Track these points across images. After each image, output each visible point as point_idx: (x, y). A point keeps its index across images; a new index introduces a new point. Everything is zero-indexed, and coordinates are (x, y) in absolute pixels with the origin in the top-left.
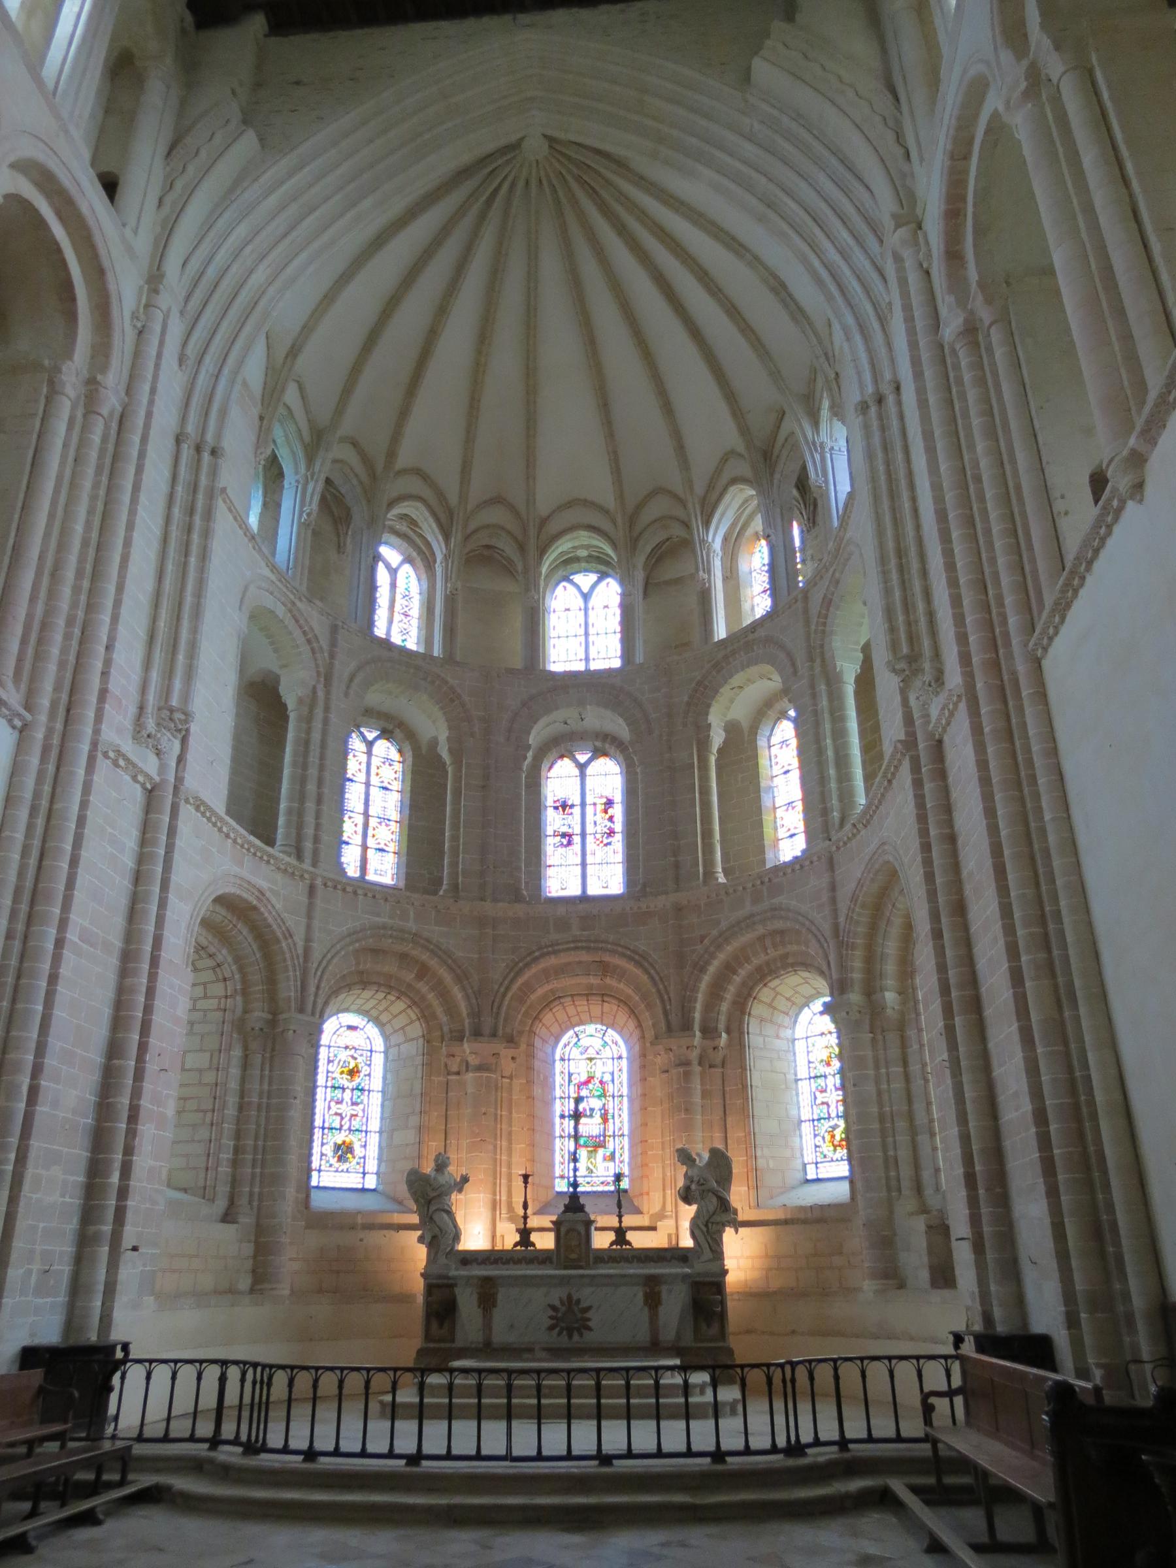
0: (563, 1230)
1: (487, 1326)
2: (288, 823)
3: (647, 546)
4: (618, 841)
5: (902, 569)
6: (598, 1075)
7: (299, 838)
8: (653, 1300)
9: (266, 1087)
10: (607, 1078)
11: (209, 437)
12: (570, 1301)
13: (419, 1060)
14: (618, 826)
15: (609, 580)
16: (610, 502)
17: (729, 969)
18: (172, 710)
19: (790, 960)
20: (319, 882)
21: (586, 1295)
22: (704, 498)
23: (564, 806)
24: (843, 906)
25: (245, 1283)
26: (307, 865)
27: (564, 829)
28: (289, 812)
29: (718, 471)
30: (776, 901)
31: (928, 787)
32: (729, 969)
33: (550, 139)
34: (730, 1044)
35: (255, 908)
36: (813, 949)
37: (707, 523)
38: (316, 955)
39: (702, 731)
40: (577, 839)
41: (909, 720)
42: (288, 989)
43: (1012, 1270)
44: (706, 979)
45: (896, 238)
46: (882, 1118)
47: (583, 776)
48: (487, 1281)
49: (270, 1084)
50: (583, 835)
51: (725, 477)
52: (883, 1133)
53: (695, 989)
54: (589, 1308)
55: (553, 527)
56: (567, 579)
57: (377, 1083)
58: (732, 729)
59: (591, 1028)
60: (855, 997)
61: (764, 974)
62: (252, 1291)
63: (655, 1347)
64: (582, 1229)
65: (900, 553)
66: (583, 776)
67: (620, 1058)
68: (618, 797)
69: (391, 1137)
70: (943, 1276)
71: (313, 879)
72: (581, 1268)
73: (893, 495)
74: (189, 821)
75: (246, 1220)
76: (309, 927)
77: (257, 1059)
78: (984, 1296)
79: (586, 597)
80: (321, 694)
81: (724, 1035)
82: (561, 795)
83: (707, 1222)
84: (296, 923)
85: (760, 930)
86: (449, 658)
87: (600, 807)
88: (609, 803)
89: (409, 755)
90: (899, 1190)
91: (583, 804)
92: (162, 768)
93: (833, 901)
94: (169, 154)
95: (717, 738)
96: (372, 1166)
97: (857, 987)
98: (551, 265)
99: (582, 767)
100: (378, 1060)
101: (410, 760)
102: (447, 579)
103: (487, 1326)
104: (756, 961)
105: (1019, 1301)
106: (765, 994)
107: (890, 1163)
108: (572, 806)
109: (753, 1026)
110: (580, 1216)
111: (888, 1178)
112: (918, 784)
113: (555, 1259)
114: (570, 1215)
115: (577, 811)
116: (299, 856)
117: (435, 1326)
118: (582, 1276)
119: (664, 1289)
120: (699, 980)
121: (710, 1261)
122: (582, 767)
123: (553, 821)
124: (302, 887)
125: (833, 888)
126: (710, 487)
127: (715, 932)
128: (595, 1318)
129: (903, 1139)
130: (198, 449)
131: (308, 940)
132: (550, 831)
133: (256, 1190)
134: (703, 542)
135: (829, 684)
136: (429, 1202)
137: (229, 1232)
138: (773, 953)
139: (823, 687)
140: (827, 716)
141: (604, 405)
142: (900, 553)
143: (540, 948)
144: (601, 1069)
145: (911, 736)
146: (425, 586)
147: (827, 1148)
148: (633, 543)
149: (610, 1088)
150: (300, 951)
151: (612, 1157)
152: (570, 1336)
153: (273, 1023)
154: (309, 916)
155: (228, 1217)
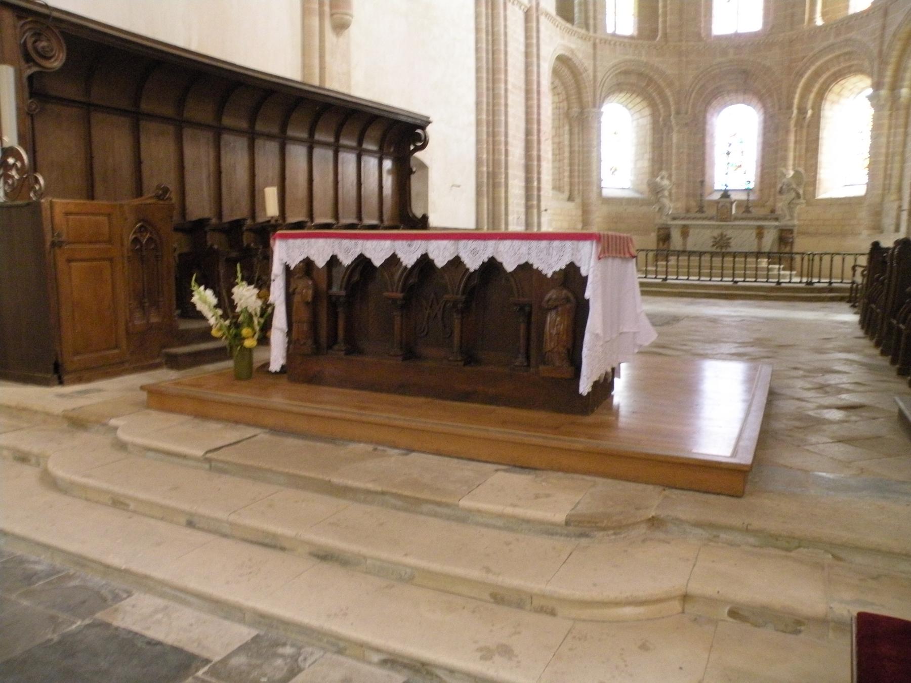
0: (720, 205)
1: (685, 244)
2: (580, 12)
7: (587, 19)
9: (581, 143)
12: (722, 236)
17: (817, 74)
19: (853, 69)
20: (598, 41)
21: (729, 233)
24: (888, 38)
26: (591, 33)
32: (817, 74)
34: (813, 115)
35: (570, 59)
36: (866, 64)
38: (599, 79)
42: (588, 98)
44: (803, 81)
46: (887, 155)
49: (583, 142)
52: (887, 162)
53: (796, 87)
54: (730, 239)
60: (884, 92)
61: (838, 76)
63: (758, 254)
64: (728, 205)
71: (595, 39)
72: (727, 221)
74: (545, 24)
75: (578, 200)
76: (595, 66)
77: (576, 130)
83: (789, 204)
84: (588, 63)
85: (837, 53)
90: (889, 189)
97: (887, 87)
103: (685, 244)
106: (836, 88)
107: (887, 176)
110: (727, 200)
111: (884, 185)
113: (715, 218)
114: (723, 200)
117: (661, 244)
118: (728, 225)
119: (766, 232)
120: (798, 82)
121: (789, 220)
127: (811, 54)
128: (733, 243)
129: (897, 166)
131: (595, 71)
133: (581, 188)
136: (658, 193)
137: (571, 205)
138: (843, 65)
143: (711, 66)
150: (591, 77)
152: (721, 249)
153: (582, 113)
154: (595, 58)
155: (570, 199)
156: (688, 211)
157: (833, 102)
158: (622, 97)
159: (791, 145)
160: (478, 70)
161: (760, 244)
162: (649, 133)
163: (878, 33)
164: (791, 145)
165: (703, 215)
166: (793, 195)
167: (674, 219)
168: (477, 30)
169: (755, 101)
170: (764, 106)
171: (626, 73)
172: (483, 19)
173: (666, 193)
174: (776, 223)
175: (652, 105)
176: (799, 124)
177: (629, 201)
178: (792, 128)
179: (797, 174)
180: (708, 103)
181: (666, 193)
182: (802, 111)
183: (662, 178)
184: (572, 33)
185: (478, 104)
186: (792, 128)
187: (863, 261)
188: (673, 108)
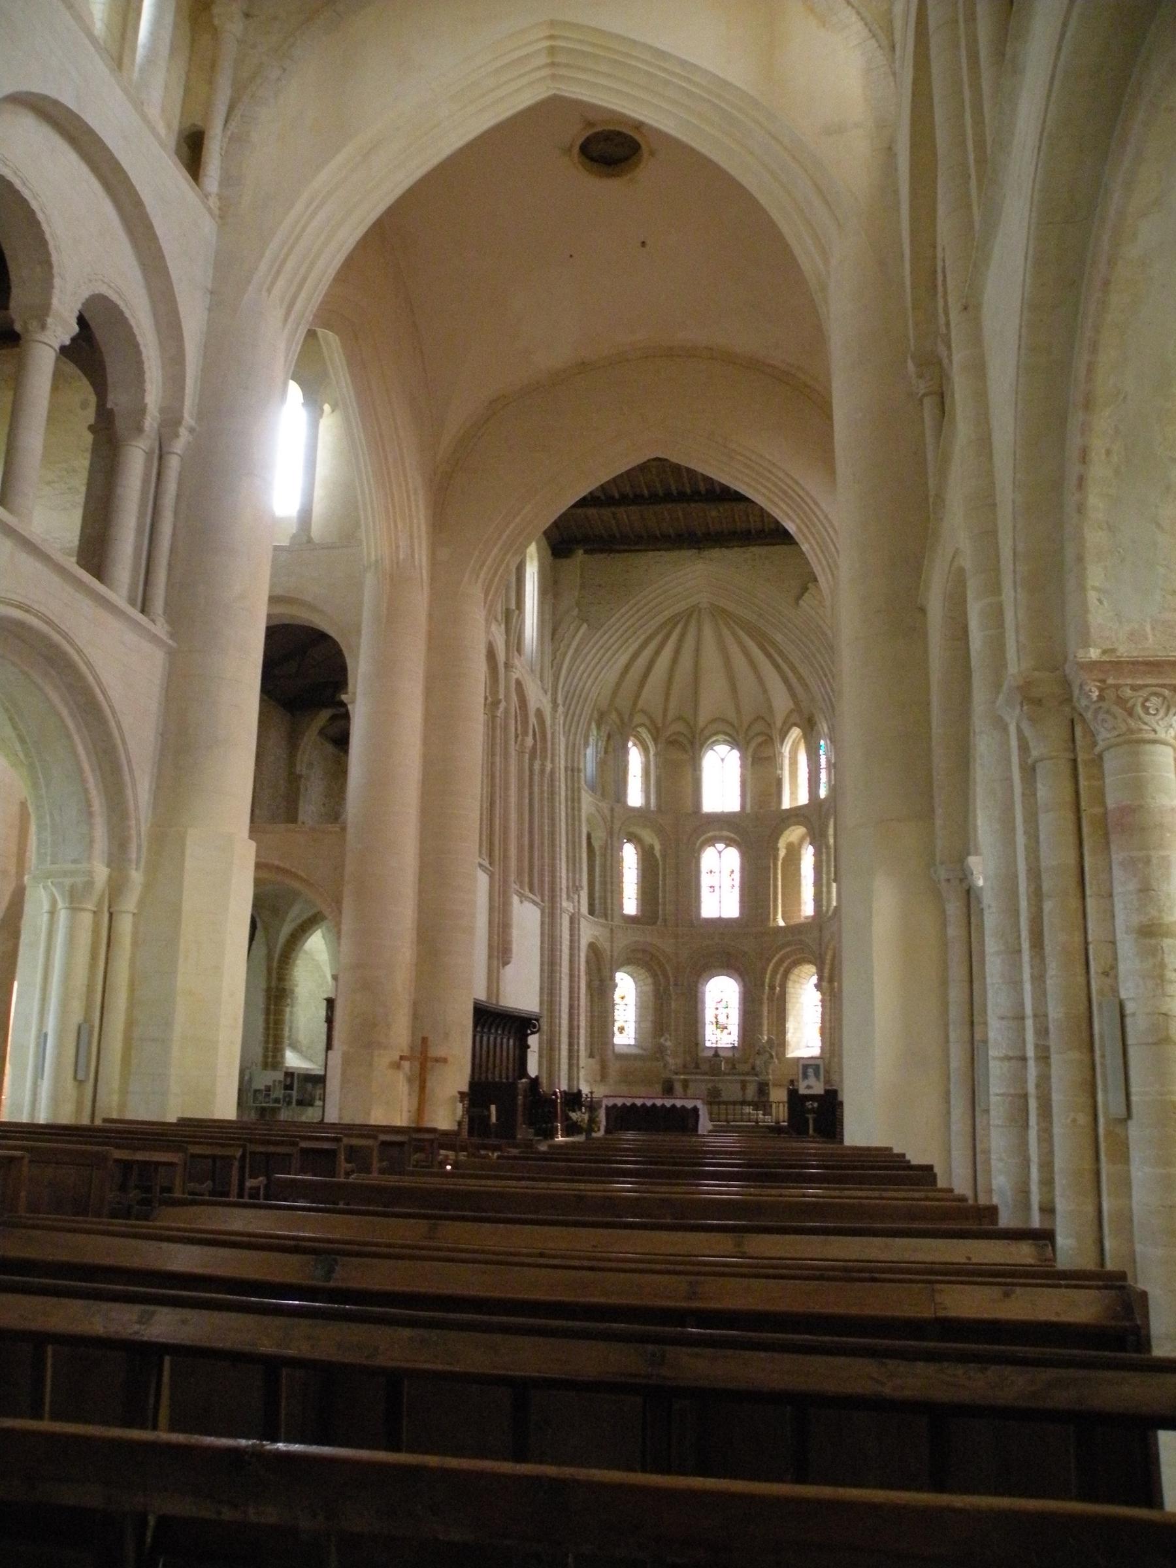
3: (753, 745)
7: (606, 909)
8: (744, 1088)
11: (576, 765)
13: (650, 994)
17: (781, 961)
18: (577, 887)
21: (720, 1086)
22: (782, 729)
25: (598, 1078)
28: (600, 898)
29: (788, 716)
32: (781, 961)
33: (712, 604)
34: (780, 991)
38: (615, 957)
40: (717, 889)
46: (830, 1028)
51: (792, 720)
55: (706, 733)
56: (712, 749)
61: (797, 963)
62: (601, 1081)
63: (744, 1103)
74: (583, 923)
75: (598, 1057)
76: (612, 946)
80: (609, 842)
81: (778, 988)
84: (607, 945)
86: (659, 806)
88: (732, 872)
89: (639, 850)
92: (574, 906)
93: (820, 944)
94: (552, 639)
95: (782, 853)
99: (720, 852)
102: (657, 767)
104: (792, 959)
109: (790, 984)
115: (717, 874)
116: (607, 920)
122: (720, 852)
124: (608, 930)
125: (820, 939)
126: (784, 723)
130: (572, 770)
131: (612, 951)
134: (780, 753)
148: (748, 743)
150: (609, 957)
154: (612, 942)
156: (685, 1066)
158: (630, 968)
159: (766, 1014)
160: (542, 964)
161: (744, 1094)
162: (652, 998)
164: (766, 1014)
165: (698, 1071)
166: (768, 1055)
167: (676, 1074)
168: (542, 934)
169: (736, 976)
170: (743, 980)
171: (633, 951)
172: (546, 927)
173: (669, 1052)
175: (654, 976)
176: (770, 999)
177: (635, 1057)
178: (766, 1001)
179: (770, 1039)
180: (699, 976)
181: (669, 1052)
182: (772, 988)
183: (666, 1040)
184: (596, 923)
185: (541, 989)
186: (766, 1001)
188: (672, 979)
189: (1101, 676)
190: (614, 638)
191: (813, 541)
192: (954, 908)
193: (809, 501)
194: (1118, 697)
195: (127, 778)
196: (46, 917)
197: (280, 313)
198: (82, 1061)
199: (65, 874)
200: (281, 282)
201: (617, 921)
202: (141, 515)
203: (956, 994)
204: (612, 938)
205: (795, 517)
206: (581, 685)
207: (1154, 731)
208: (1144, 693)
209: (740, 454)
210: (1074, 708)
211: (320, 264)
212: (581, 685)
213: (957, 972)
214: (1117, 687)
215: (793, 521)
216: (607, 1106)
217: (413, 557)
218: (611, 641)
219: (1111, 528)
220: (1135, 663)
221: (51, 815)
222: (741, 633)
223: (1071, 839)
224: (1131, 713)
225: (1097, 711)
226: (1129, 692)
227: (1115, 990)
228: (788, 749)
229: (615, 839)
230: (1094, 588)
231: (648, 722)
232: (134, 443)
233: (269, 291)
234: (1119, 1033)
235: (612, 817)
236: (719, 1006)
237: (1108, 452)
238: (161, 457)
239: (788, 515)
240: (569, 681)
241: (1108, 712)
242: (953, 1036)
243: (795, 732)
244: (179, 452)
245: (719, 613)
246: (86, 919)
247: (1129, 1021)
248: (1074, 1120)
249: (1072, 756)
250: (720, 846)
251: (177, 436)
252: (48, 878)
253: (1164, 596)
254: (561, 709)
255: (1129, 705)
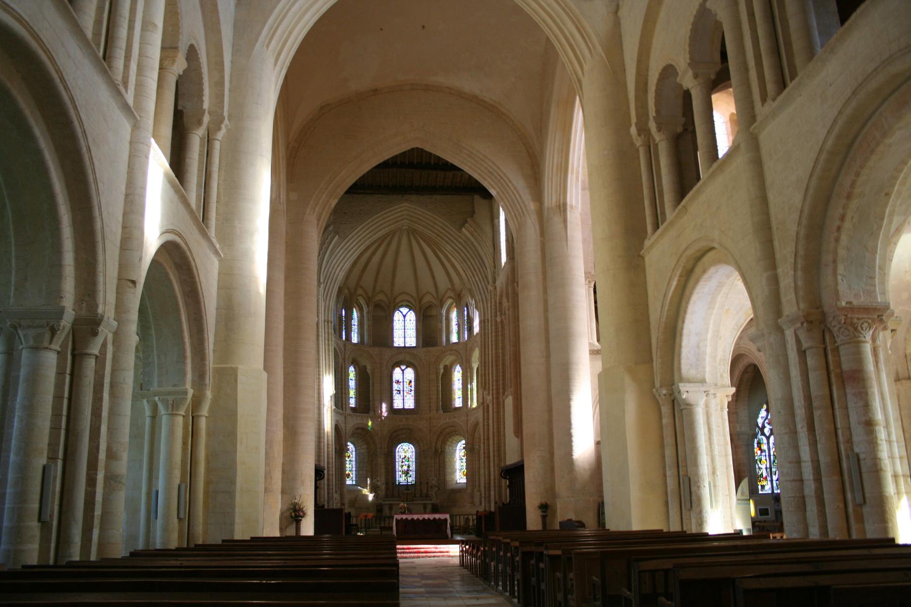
4: (413, 393)
5: (485, 366)
6: (407, 456)
7: (342, 404)
10: (410, 457)
14: (413, 389)
15: (411, 311)
16: (414, 295)
23: (398, 382)
27: (398, 389)
30: (454, 420)
31: (485, 414)
37: (442, 308)
39: (437, 369)
40: (402, 392)
41: (483, 398)
43: (490, 502)
45: (490, 288)
47: (403, 373)
48: (391, 504)
50: (403, 391)
51: (447, 295)
57: (354, 459)
58: (446, 367)
59: (406, 444)
65: (485, 362)
66: (403, 373)
67: (413, 452)
68: (413, 380)
69: (359, 472)
70: (481, 503)
73: (485, 348)
75: (339, 492)
76: (345, 427)
78: (485, 506)
79: (404, 316)
80: (343, 365)
82: (397, 379)
84: (343, 426)
87: (408, 383)
88: (410, 382)
89: (357, 369)
91: (403, 382)
93: (467, 424)
96: (354, 479)
98: (404, 241)
100: (354, 453)
101: (358, 371)
105: (490, 507)
108: (400, 382)
112: (484, 412)
115: (402, 384)
122: (403, 371)
123: (395, 386)
124: (343, 417)
125: (467, 421)
130: (328, 322)
131: (345, 430)
132: (394, 389)
135: (470, 369)
136: (376, 488)
139: (469, 370)
140: (469, 378)
141: (415, 270)
142: (485, 362)
144: (409, 455)
145: (483, 401)
146: (359, 315)
147: (462, 476)
149: (410, 459)
151: (411, 476)
157: (449, 446)
163: (465, 422)
171: (358, 428)
174: (431, 502)
183: (378, 481)
187: (475, 517)
189: (846, 313)
190: (354, 243)
191: (506, 201)
192: (666, 410)
193: (505, 178)
194: (851, 322)
195: (206, 336)
196: (148, 421)
197: (272, 60)
198: (182, 507)
199: (169, 393)
200: (273, 43)
201: (349, 411)
202: (199, 176)
203: (669, 452)
204: (345, 422)
205: (495, 186)
206: (333, 271)
207: (865, 337)
208: (862, 321)
209: (467, 150)
210: (826, 326)
211: (295, 33)
212: (333, 271)
213: (669, 440)
214: (852, 318)
215: (494, 189)
216: (396, 519)
217: (280, 198)
218: (352, 245)
219: (849, 249)
220: (859, 308)
221: (159, 357)
222: (423, 244)
223: (826, 383)
224: (856, 329)
225: (840, 328)
226: (855, 321)
227: (852, 450)
228: (445, 311)
229: (346, 363)
230: (840, 274)
231: (364, 295)
232: (194, 132)
233: (268, 46)
234: (857, 468)
235: (345, 349)
236: (404, 460)
237: (852, 217)
238: (208, 141)
239: (491, 185)
240: (326, 269)
241: (846, 329)
242: (668, 473)
243: (450, 301)
244: (220, 139)
245: (412, 232)
246: (180, 420)
247: (862, 462)
248: (838, 506)
249: (823, 346)
250: (403, 367)
251: (219, 129)
252: (156, 396)
253: (867, 279)
254: (322, 286)
255: (856, 326)
